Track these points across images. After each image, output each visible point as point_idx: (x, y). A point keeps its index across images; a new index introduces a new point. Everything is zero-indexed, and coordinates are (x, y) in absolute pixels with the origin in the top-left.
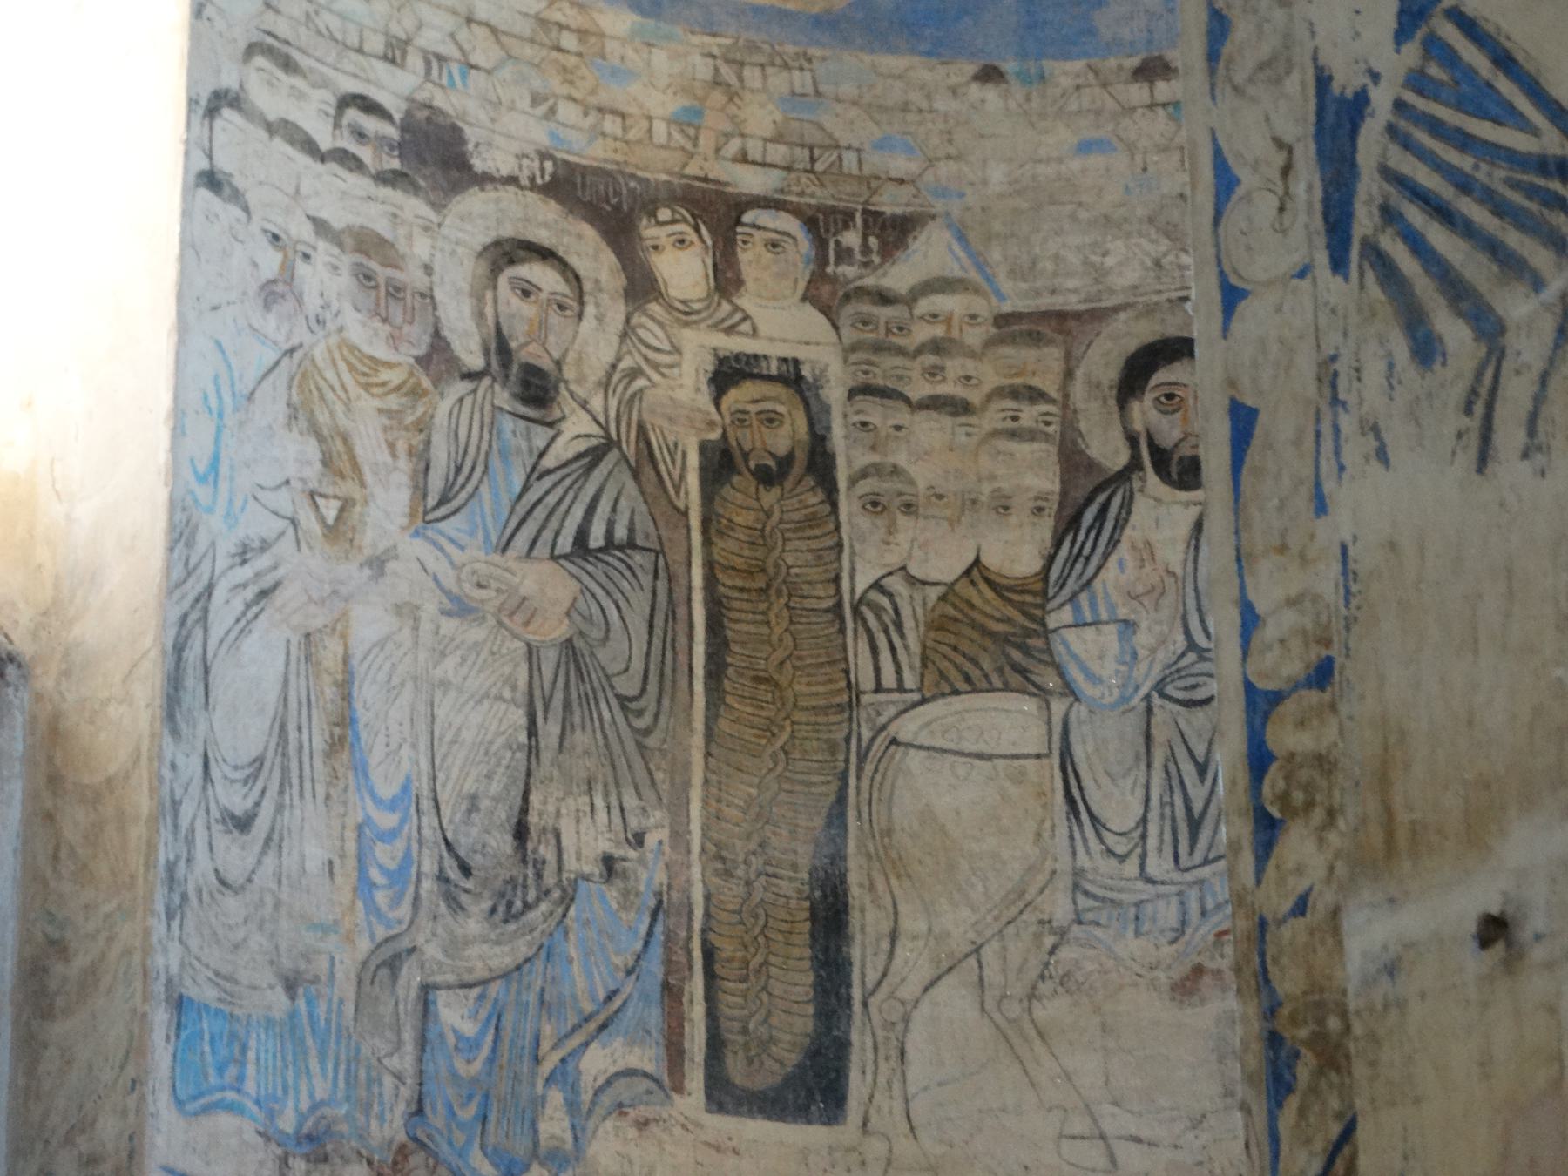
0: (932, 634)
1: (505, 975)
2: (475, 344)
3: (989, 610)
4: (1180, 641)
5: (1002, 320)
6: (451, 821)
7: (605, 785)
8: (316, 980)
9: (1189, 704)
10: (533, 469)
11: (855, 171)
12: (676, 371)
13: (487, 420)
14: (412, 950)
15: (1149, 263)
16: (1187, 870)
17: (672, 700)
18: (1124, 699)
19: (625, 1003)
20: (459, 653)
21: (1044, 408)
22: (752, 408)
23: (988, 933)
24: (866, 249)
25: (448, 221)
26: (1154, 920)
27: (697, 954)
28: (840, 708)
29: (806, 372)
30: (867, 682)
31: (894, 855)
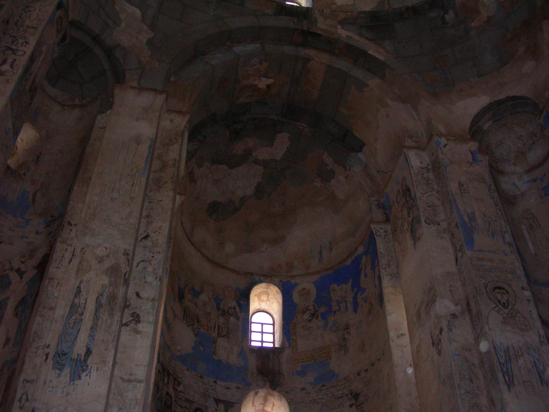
5: (186, 398)
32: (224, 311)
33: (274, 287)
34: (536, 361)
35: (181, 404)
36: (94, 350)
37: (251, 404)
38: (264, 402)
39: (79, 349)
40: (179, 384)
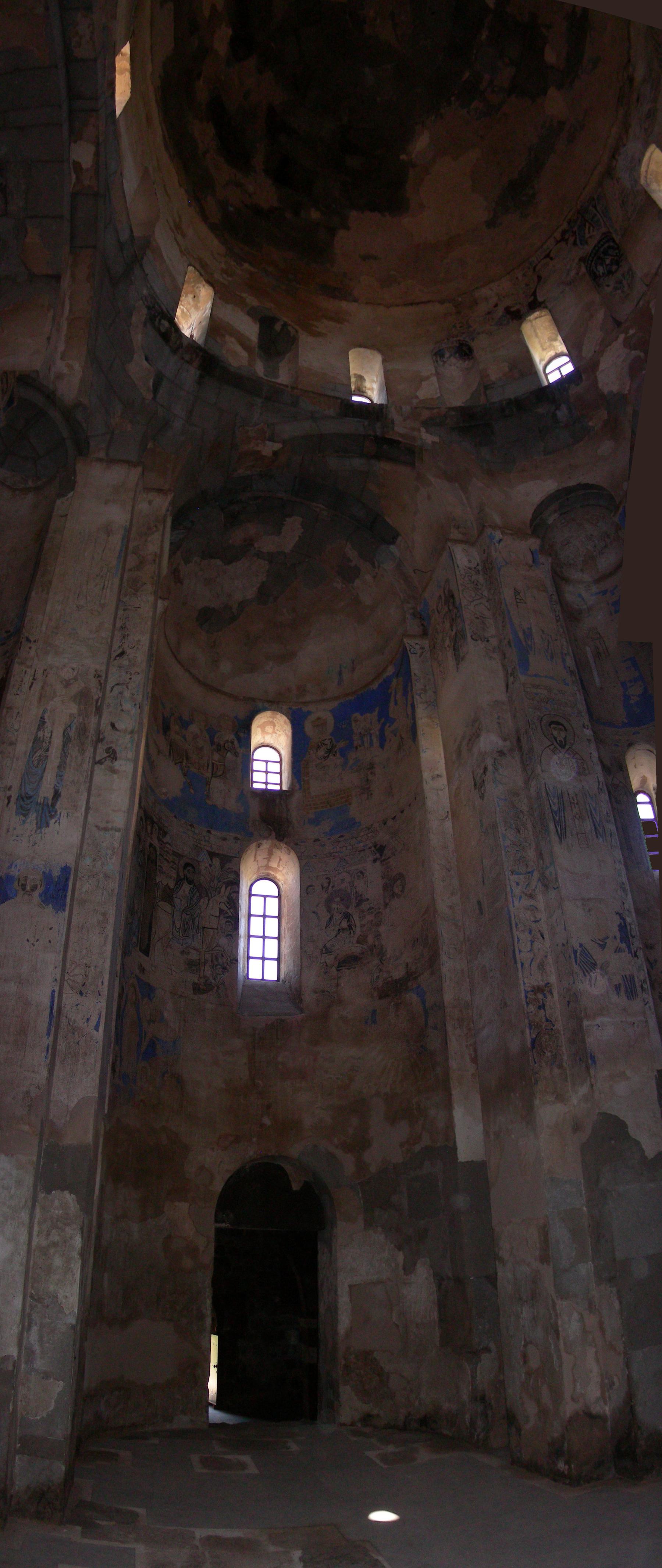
5: (174, 852)
9: (186, 914)
32: (218, 745)
33: (281, 716)
34: (593, 811)
36: (63, 793)
37: (252, 858)
38: (268, 857)
39: (46, 791)
40: (165, 833)
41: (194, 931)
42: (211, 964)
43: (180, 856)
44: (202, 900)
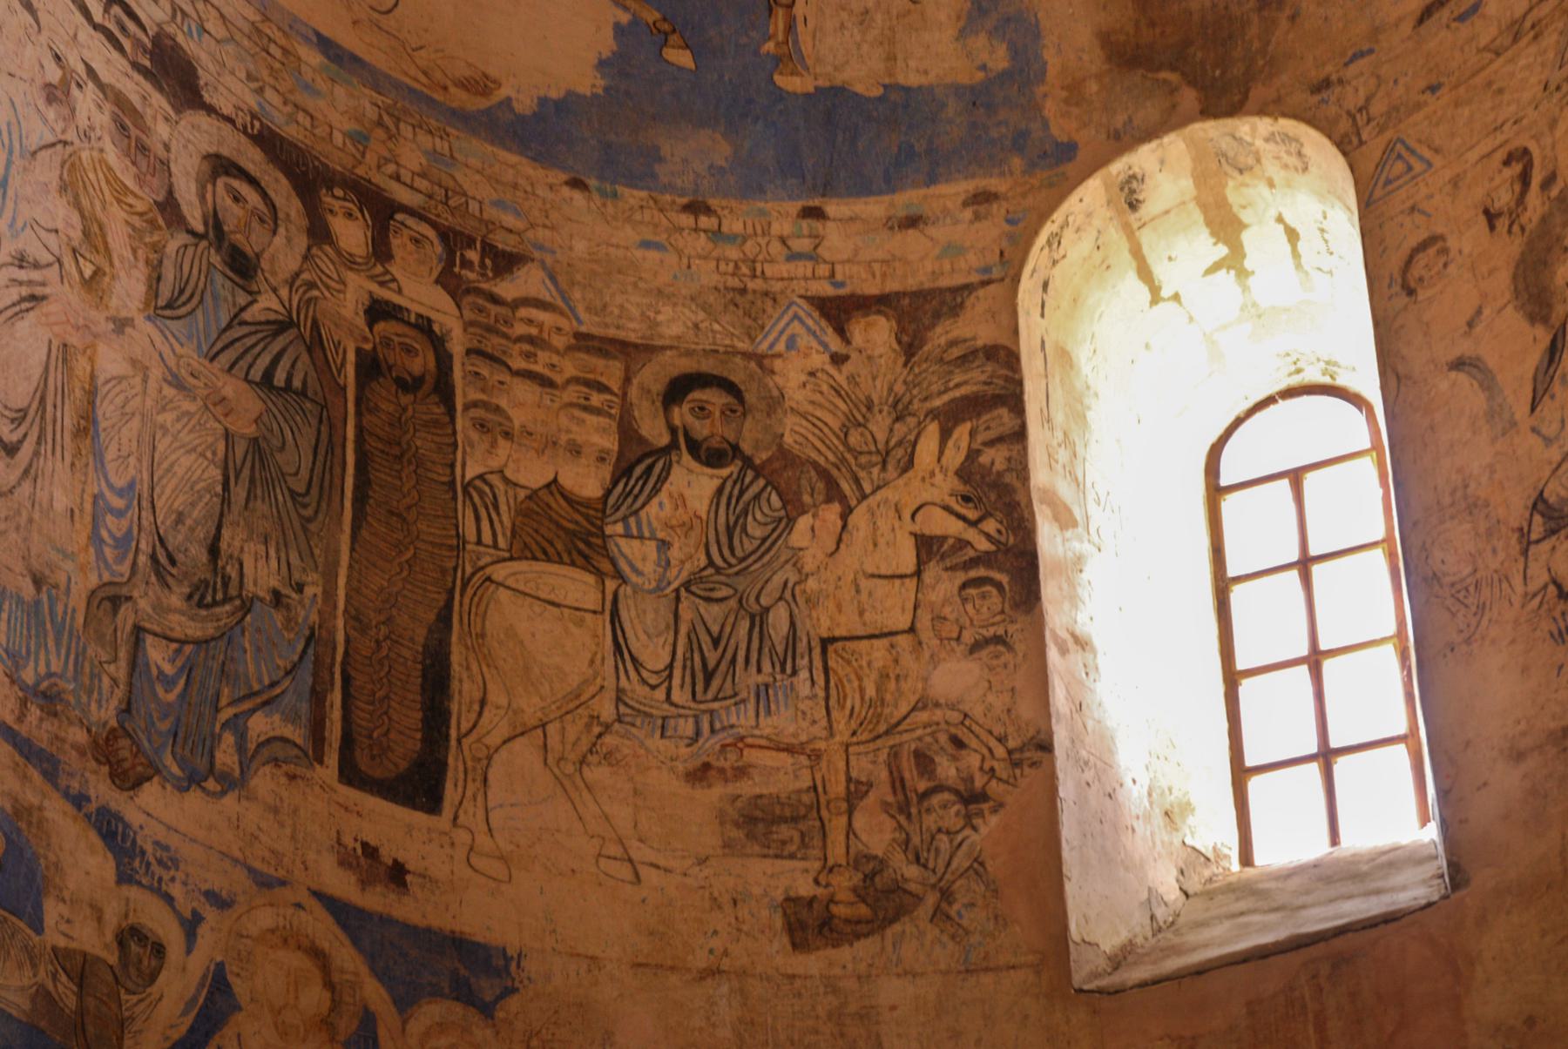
0: (520, 518)
1: (197, 642)
2: (198, 213)
3: (563, 513)
4: (703, 561)
5: (578, 336)
6: (163, 523)
7: (277, 543)
8: (56, 586)
9: (708, 600)
10: (236, 316)
11: (477, 214)
12: (342, 296)
13: (204, 268)
14: (129, 598)
15: (690, 324)
16: (701, 702)
17: (328, 505)
18: (659, 588)
19: (283, 692)
20: (175, 413)
21: (609, 397)
22: (396, 339)
23: (552, 717)
24: (483, 265)
25: (183, 123)
26: (676, 730)
27: (338, 676)
28: (451, 548)
29: (436, 328)
30: (471, 534)
31: (486, 652)
35: (538, 368)
40: (506, 262)
41: (767, 667)
42: (890, 799)
43: (629, 352)
44: (804, 522)
